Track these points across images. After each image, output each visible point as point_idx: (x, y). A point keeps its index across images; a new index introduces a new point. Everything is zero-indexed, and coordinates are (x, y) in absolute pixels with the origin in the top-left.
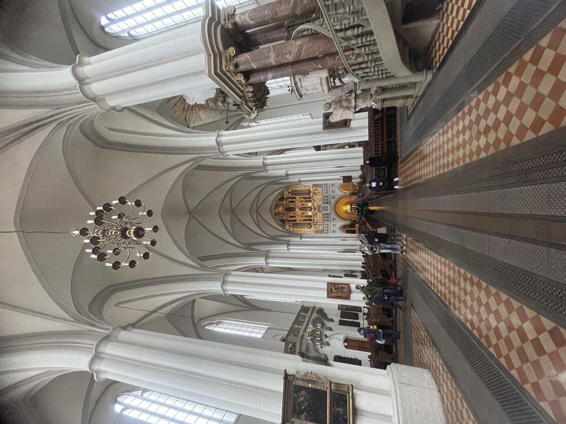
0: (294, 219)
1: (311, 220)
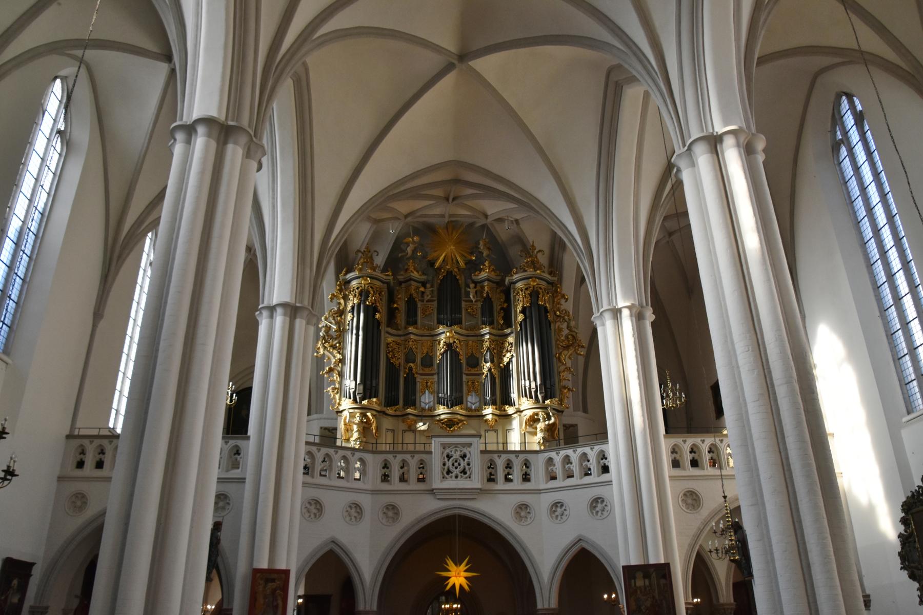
0: (401, 318)
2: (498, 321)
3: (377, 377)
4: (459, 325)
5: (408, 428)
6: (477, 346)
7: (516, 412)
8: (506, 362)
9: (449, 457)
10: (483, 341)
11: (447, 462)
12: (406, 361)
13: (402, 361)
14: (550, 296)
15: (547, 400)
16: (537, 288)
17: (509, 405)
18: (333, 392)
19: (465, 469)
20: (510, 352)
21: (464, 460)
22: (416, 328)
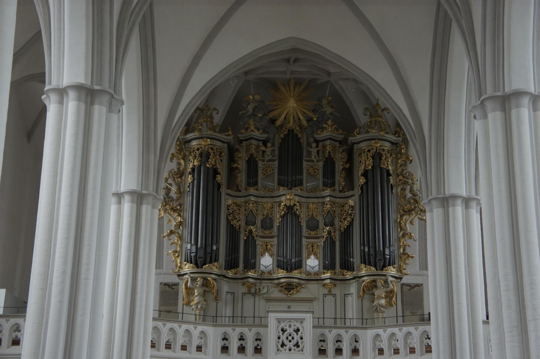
0: (242, 178)
1: (231, 264)
2: (339, 182)
3: (218, 242)
4: (300, 187)
5: (248, 291)
6: (318, 208)
7: (354, 278)
8: (346, 226)
9: (283, 331)
10: (324, 203)
11: (282, 336)
12: (246, 223)
13: (243, 223)
14: (393, 157)
15: (385, 267)
16: (380, 149)
17: (348, 270)
18: (174, 255)
19: (298, 343)
20: (351, 215)
21: (297, 334)
22: (257, 190)
